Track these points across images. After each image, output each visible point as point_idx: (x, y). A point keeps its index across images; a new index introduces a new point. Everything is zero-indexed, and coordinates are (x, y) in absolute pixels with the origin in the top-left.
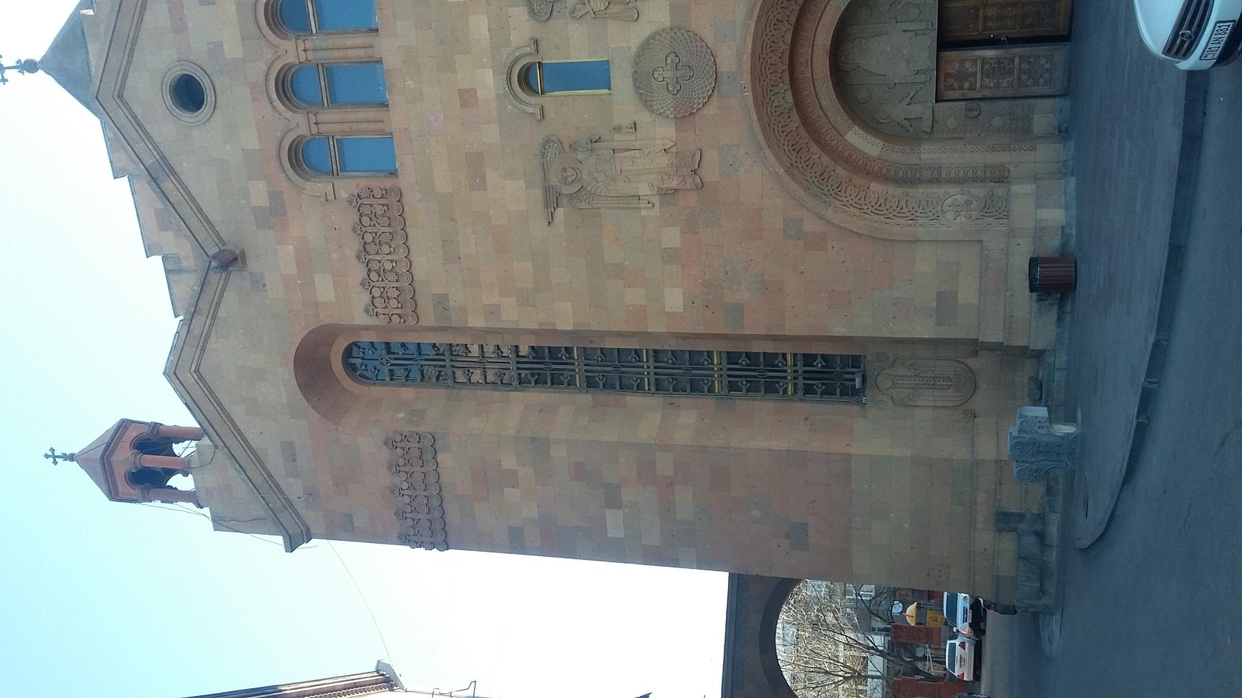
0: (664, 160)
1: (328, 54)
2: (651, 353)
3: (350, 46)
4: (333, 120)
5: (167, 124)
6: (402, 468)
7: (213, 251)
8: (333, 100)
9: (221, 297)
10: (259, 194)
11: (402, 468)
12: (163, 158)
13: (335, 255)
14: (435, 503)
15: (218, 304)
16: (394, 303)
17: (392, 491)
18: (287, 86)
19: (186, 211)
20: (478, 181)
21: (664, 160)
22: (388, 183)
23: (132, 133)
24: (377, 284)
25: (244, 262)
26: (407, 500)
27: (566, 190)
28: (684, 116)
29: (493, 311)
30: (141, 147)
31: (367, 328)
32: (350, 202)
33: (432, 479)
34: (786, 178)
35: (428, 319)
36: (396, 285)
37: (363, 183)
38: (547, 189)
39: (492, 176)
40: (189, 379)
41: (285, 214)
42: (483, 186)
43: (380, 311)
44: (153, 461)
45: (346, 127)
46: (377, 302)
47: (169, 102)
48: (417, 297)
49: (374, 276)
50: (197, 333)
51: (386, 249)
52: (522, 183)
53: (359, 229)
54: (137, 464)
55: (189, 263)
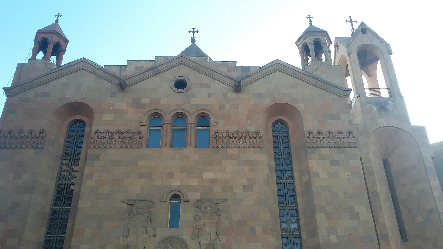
1: (189, 130)
2: (63, 238)
3: (191, 137)
6: (30, 135)
7: (127, 82)
8: (174, 130)
9: (109, 82)
10: (145, 101)
11: (30, 135)
12: (160, 73)
13: (120, 122)
14: (13, 145)
15: (107, 80)
16: (99, 140)
17: (21, 130)
20: (141, 176)
22: (144, 144)
23: (170, 65)
24: (107, 135)
25: (121, 92)
26: (17, 135)
27: (134, 208)
29: (90, 176)
30: (165, 66)
31: (91, 129)
32: (139, 130)
33: (24, 145)
35: (91, 152)
36: (106, 142)
37: (145, 136)
38: (135, 201)
40: (81, 65)
43: (96, 135)
44: (50, 48)
45: (165, 133)
47: (178, 78)
48: (100, 149)
49: (110, 135)
50: (98, 71)
51: (120, 140)
52: (139, 192)
53: (128, 132)
54: (50, 41)
55: (123, 74)
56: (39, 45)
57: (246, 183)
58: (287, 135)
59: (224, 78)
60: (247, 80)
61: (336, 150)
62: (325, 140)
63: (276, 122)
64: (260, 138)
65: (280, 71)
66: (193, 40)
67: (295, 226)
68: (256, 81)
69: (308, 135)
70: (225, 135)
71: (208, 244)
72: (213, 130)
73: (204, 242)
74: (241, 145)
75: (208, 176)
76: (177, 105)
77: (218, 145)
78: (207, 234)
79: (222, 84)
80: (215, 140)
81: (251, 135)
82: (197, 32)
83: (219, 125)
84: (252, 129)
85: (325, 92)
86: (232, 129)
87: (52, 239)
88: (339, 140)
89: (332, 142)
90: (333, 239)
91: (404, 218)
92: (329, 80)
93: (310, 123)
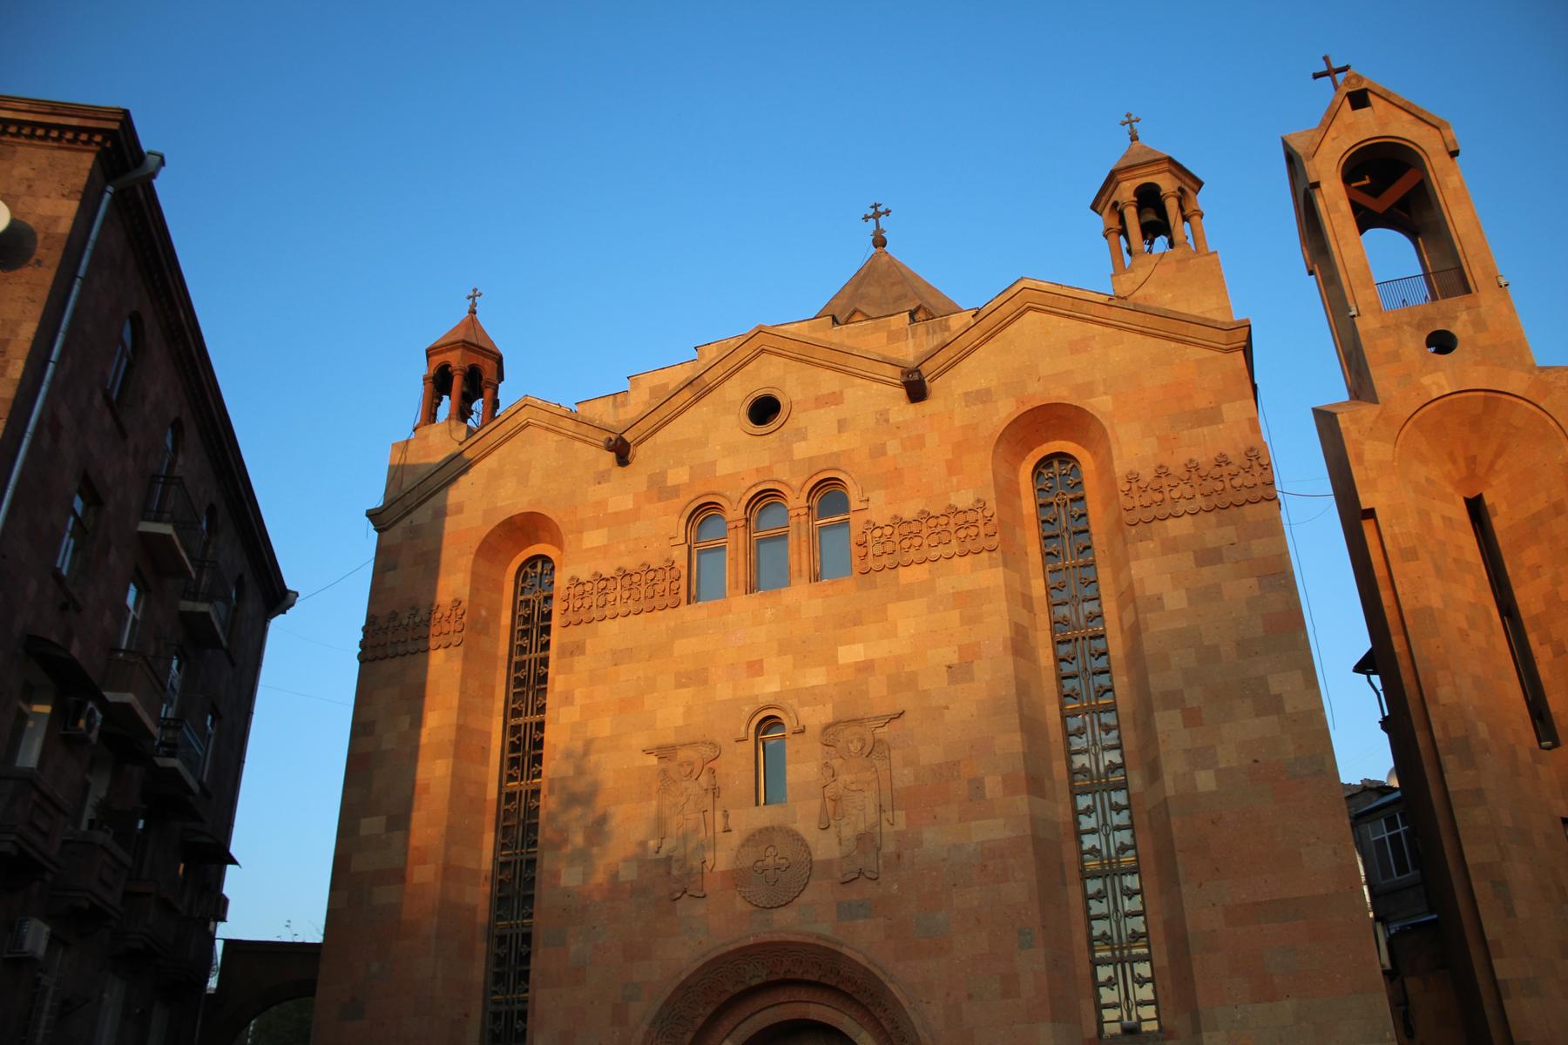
0: (696, 863)
4: (736, 542)
5: (739, 392)
7: (628, 437)
10: (678, 476)
12: (711, 390)
13: (622, 547)
14: (401, 649)
16: (578, 604)
18: (766, 498)
19: (665, 411)
20: (684, 680)
21: (696, 863)
23: (731, 363)
28: (736, 878)
29: (568, 699)
30: (719, 370)
34: (677, 982)
38: (673, 747)
39: (686, 694)
40: (522, 417)
41: (660, 500)
42: (680, 685)
43: (572, 591)
46: (580, 588)
47: (757, 395)
49: (603, 584)
52: (680, 723)
56: (430, 386)
57: (954, 658)
58: (1080, 494)
59: (877, 367)
60: (941, 358)
61: (1212, 517)
62: (1175, 494)
63: (1046, 461)
64: (988, 520)
65: (1037, 310)
66: (880, 242)
67: (1114, 757)
68: (968, 354)
69: (1127, 487)
70: (888, 531)
71: (860, 838)
72: (857, 522)
73: (848, 832)
74: (934, 553)
75: (851, 654)
76: (757, 470)
77: (871, 563)
78: (855, 812)
79: (875, 385)
80: (863, 551)
81: (961, 518)
82: (887, 212)
83: (873, 505)
84: (964, 499)
85: (1173, 344)
86: (910, 511)
87: (512, 858)
88: (1219, 486)
89: (1198, 496)
90: (1205, 781)
91: (1544, 672)
92: (1181, 308)
93: (1132, 448)
